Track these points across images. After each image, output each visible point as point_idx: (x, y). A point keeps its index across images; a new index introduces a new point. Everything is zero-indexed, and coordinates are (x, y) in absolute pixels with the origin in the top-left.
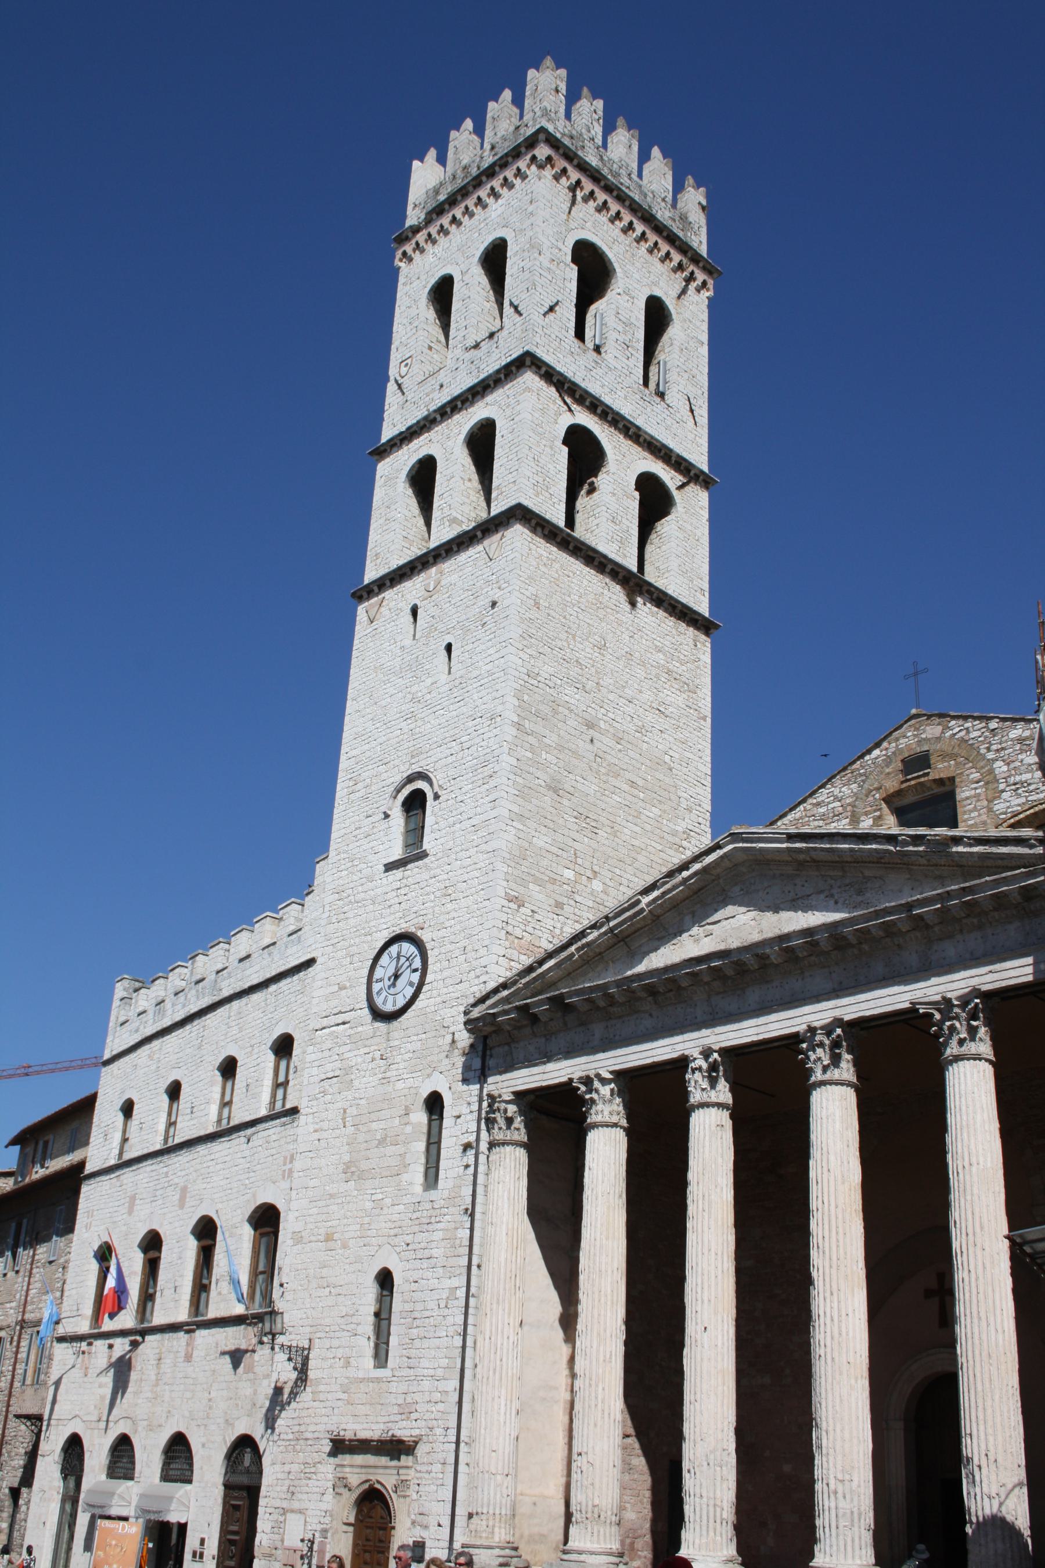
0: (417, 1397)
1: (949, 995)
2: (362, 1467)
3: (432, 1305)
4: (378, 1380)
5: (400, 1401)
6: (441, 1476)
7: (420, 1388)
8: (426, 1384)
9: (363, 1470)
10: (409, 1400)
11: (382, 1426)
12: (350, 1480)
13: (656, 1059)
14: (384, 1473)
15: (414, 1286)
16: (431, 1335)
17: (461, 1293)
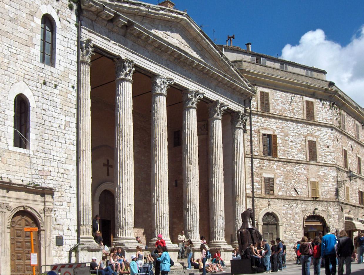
0: (51, 169)
1: (220, 100)
2: (17, 199)
3: (57, 126)
4: (24, 155)
5: (40, 168)
6: (68, 208)
7: (52, 165)
8: (54, 164)
9: (18, 201)
10: (46, 169)
11: (29, 180)
12: (10, 205)
13: (151, 70)
14: (35, 203)
15: (43, 112)
16: (57, 140)
17: (74, 125)
